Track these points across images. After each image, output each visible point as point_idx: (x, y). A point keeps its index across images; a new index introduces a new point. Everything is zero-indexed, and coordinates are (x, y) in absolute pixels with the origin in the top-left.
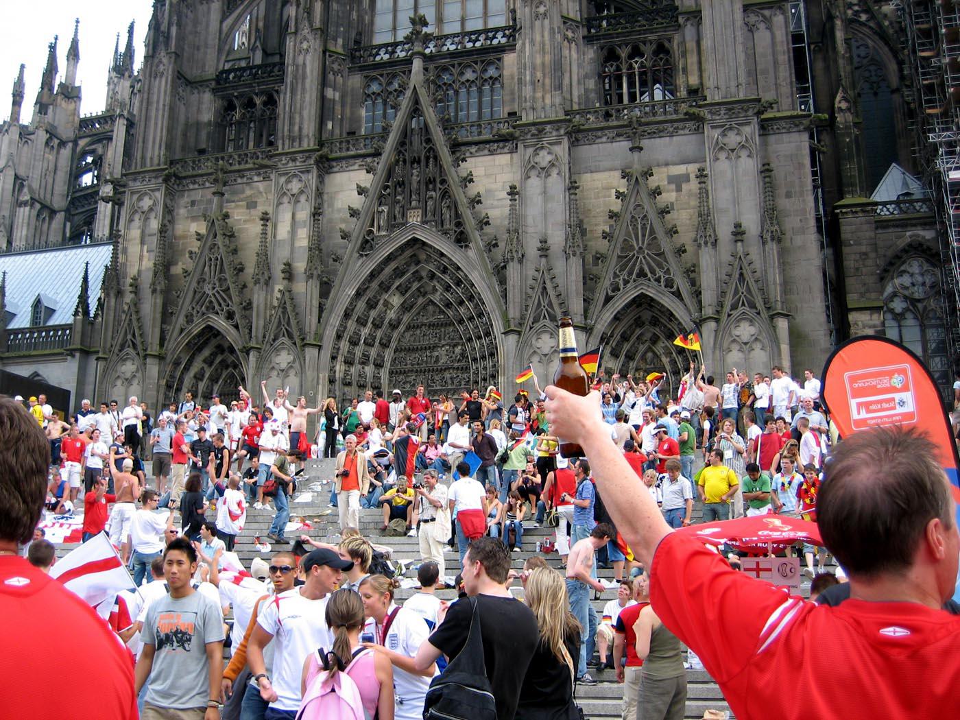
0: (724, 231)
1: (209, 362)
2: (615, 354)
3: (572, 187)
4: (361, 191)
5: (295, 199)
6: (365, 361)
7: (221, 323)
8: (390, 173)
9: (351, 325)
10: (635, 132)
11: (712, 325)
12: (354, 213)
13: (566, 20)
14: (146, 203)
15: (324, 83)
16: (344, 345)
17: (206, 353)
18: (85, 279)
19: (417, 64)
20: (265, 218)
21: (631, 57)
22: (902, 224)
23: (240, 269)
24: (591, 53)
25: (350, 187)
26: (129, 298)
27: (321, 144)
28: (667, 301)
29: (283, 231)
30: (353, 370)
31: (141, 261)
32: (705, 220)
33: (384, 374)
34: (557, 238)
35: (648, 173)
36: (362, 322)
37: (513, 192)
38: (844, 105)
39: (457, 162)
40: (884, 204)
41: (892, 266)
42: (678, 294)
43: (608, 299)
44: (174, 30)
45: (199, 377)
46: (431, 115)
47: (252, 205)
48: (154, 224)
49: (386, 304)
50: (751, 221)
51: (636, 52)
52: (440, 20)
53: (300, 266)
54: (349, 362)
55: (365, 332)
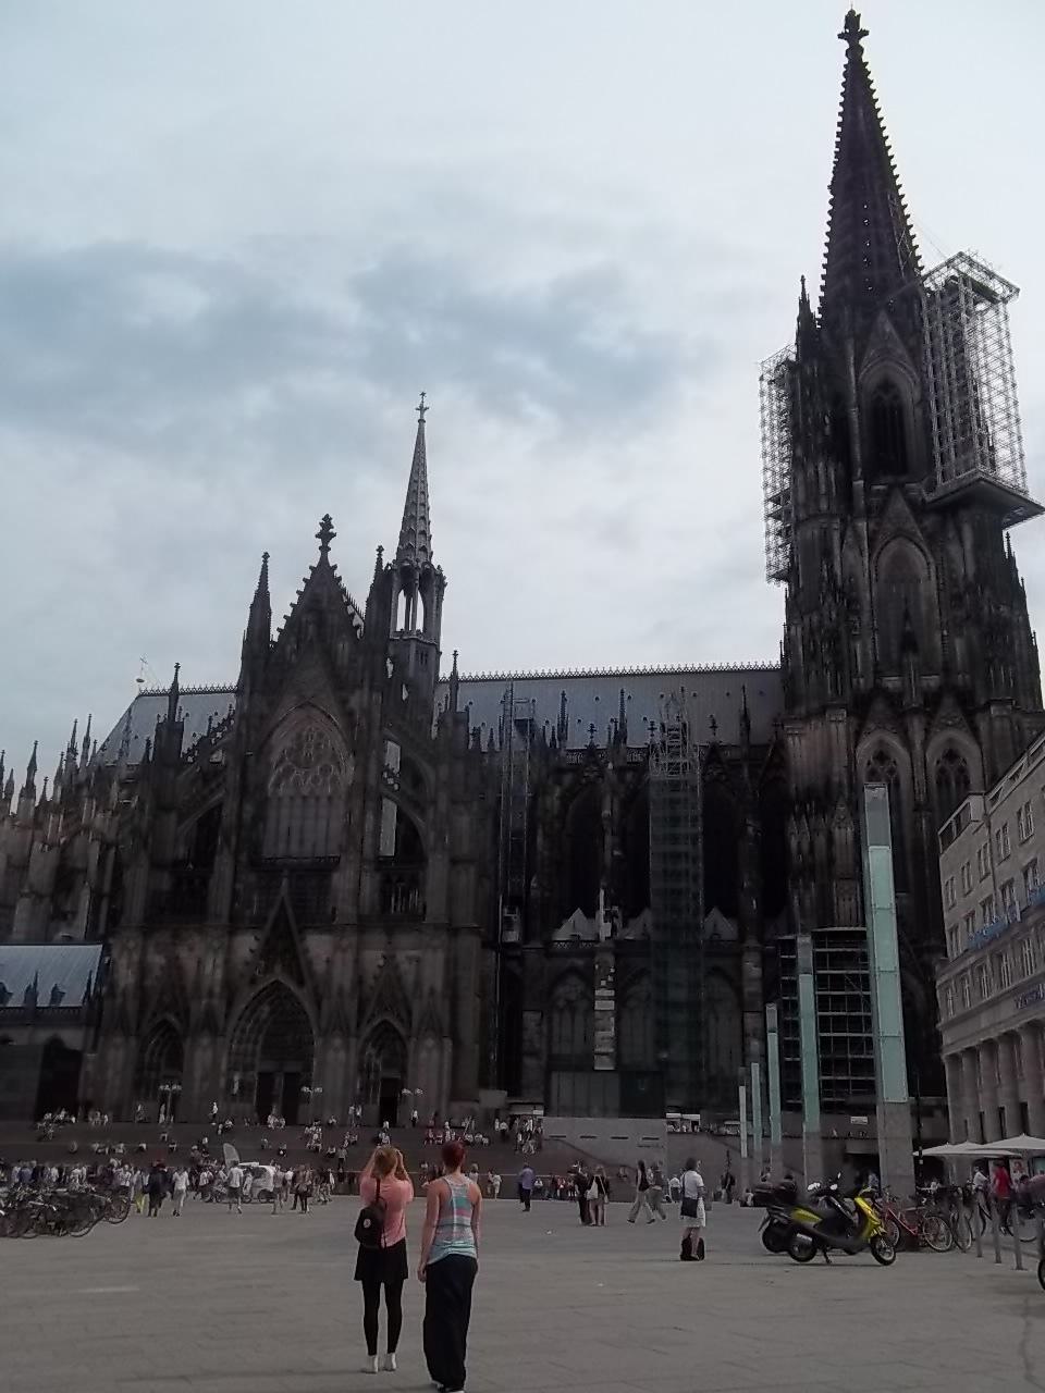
0: (426, 989)
1: (163, 1035)
2: (374, 1046)
3: (357, 961)
4: (251, 951)
5: (216, 951)
6: (248, 1041)
7: (172, 1019)
8: (267, 942)
9: (243, 1022)
10: (390, 931)
11: (415, 1039)
12: (247, 963)
13: (363, 861)
14: (131, 944)
15: (235, 880)
16: (238, 1033)
17: (161, 1032)
18: (90, 981)
19: (285, 882)
20: (199, 962)
21: (397, 882)
22: (566, 955)
23: (183, 989)
24: (378, 877)
25: (246, 944)
26: (119, 1000)
27: (232, 918)
28: (397, 1024)
29: (209, 968)
30: (243, 1046)
31: (126, 977)
32: (418, 984)
33: (258, 1048)
34: (347, 985)
35: (394, 957)
36: (248, 1020)
37: (328, 961)
38: (535, 885)
39: (303, 939)
40: (559, 942)
41: (560, 978)
42: (402, 1021)
43: (368, 1022)
44: (150, 840)
45: (157, 1043)
46: (290, 911)
47: (191, 949)
48: (136, 957)
49: (262, 1011)
50: (439, 985)
51: (400, 880)
52: (301, 842)
53: (217, 990)
54: (239, 1042)
55: (249, 1026)
